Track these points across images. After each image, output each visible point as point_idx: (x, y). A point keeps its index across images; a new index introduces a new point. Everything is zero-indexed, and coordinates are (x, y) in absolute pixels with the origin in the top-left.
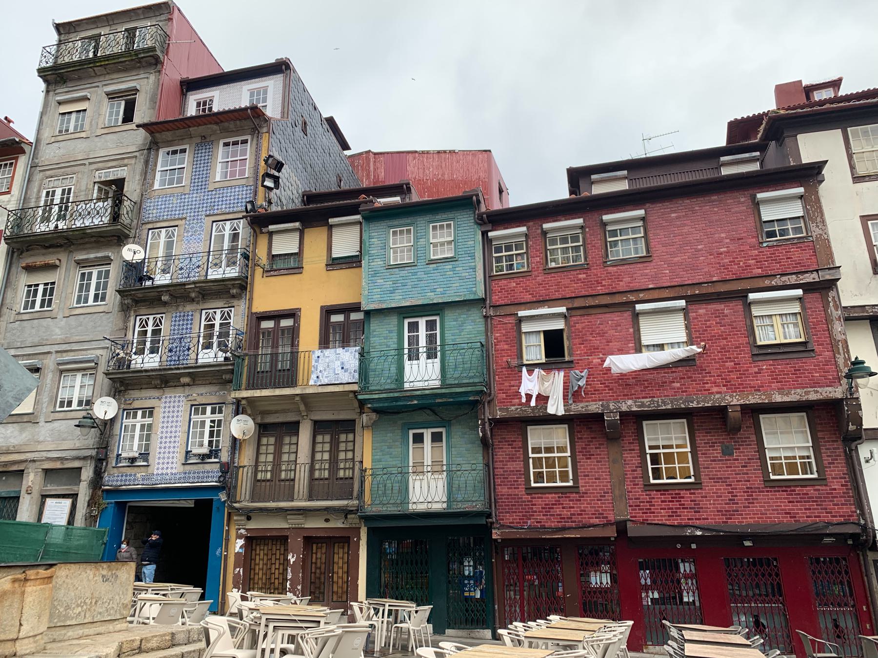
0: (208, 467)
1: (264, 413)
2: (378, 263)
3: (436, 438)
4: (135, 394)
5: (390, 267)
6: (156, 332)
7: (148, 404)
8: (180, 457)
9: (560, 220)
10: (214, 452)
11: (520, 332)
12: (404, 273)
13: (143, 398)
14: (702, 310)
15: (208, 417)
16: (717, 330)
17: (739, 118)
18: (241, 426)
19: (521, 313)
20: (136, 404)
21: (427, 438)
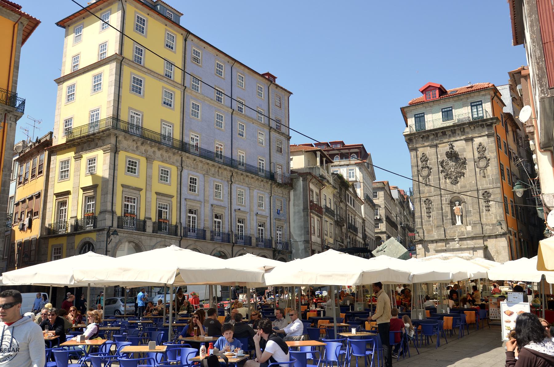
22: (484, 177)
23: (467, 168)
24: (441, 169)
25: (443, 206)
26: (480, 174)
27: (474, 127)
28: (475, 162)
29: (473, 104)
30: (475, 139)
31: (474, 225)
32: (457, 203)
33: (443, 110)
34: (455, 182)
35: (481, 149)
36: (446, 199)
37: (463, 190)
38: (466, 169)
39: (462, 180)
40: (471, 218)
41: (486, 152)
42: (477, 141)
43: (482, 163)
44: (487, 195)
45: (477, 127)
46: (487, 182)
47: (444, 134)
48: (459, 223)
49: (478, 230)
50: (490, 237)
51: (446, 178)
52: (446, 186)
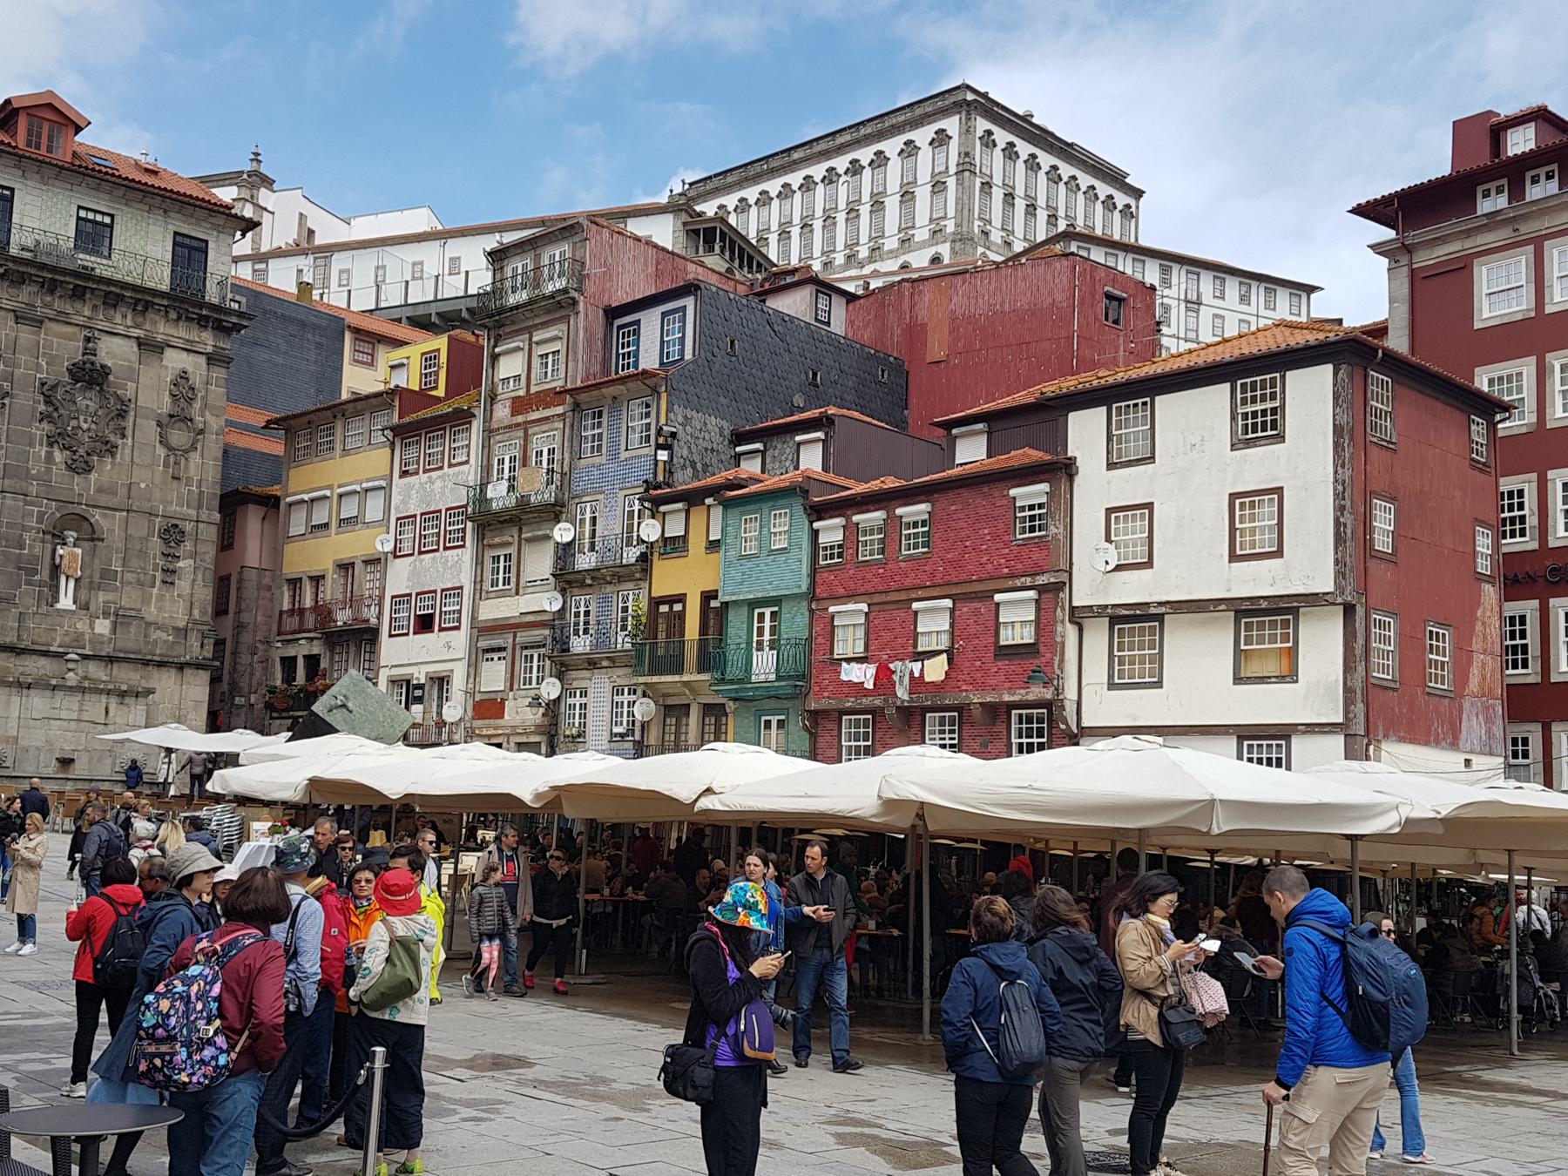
0: (626, 745)
1: (665, 695)
2: (732, 553)
3: (781, 724)
4: (574, 674)
5: (741, 558)
6: (587, 613)
7: (583, 684)
8: (606, 735)
9: (868, 511)
10: (630, 732)
11: (833, 627)
12: (749, 564)
13: (580, 679)
14: (965, 609)
15: (626, 698)
16: (972, 630)
17: (1379, 197)
18: (644, 709)
19: (832, 609)
20: (575, 684)
21: (774, 725)
22: (174, 478)
23: (129, 432)
24: (42, 407)
25: (26, 536)
26: (166, 465)
27: (179, 318)
28: (159, 424)
29: (179, 239)
30: (169, 353)
31: (120, 619)
32: (71, 536)
33: (83, 214)
34: (80, 467)
35: (182, 388)
36: (41, 515)
37: (103, 500)
38: (124, 436)
39: (105, 471)
40: (110, 596)
41: (197, 405)
42: (175, 360)
43: (178, 437)
44: (172, 534)
45: (189, 319)
46: (180, 497)
47: (78, 294)
48: (66, 602)
49: (130, 639)
50: (161, 665)
51: (51, 445)
52: (49, 470)
